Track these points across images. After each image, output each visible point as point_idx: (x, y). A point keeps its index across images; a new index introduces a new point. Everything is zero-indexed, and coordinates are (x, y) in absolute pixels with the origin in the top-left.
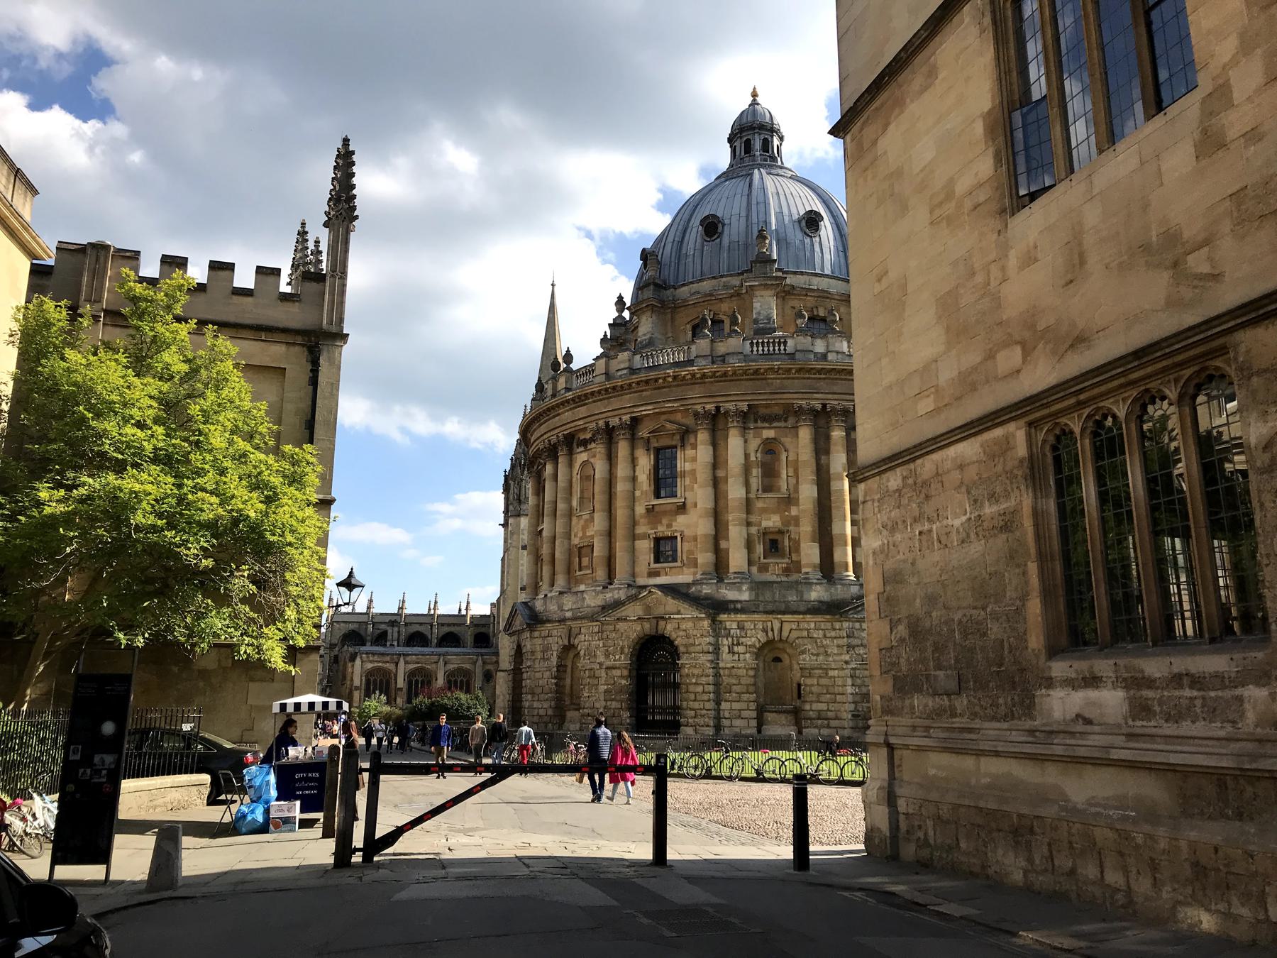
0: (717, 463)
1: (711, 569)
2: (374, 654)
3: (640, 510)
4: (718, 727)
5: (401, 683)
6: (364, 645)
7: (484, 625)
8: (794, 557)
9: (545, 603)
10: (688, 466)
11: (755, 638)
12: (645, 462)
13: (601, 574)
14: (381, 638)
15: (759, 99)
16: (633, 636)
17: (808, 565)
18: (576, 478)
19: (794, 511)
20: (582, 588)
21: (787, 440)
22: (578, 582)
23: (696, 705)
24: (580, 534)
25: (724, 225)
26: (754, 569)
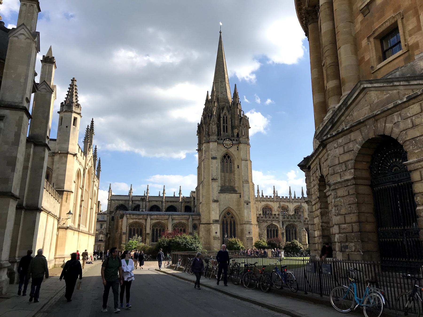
2: (133, 215)
7: (188, 202)
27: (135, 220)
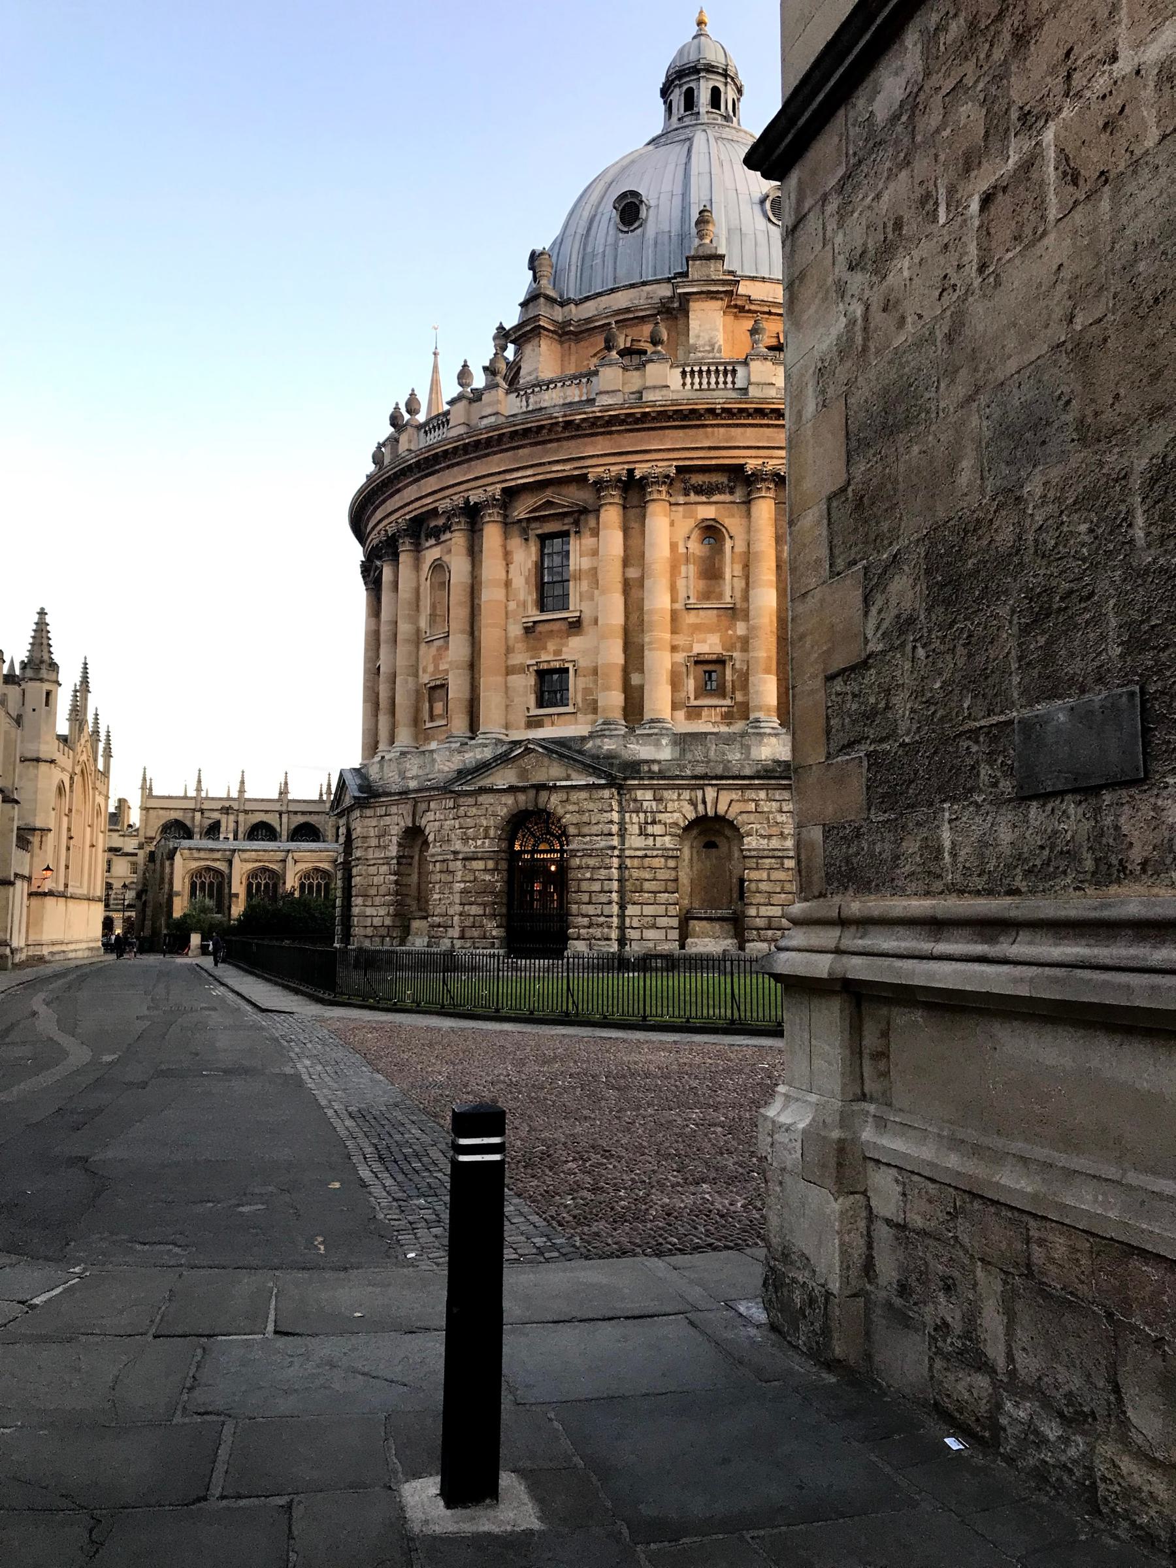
0: (634, 556)
1: (617, 715)
2: (199, 850)
3: (516, 630)
4: (622, 941)
5: (238, 887)
6: (190, 836)
8: (739, 697)
9: (382, 768)
10: (586, 563)
11: (680, 809)
12: (525, 557)
13: (459, 724)
14: (213, 830)
15: (708, 29)
16: (503, 812)
17: (759, 708)
18: (426, 586)
19: (741, 629)
20: (433, 745)
21: (733, 523)
22: (428, 739)
23: (590, 909)
24: (431, 668)
25: (648, 208)
26: (681, 714)
27: (203, 863)
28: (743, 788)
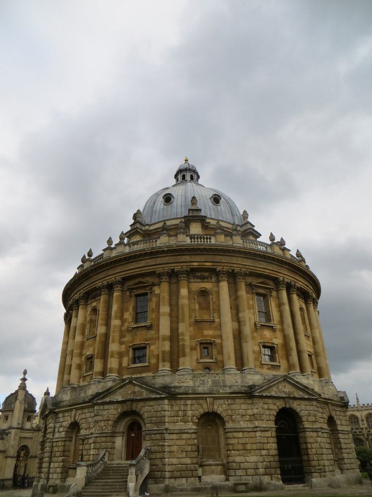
26: (81, 380)
28: (82, 408)
